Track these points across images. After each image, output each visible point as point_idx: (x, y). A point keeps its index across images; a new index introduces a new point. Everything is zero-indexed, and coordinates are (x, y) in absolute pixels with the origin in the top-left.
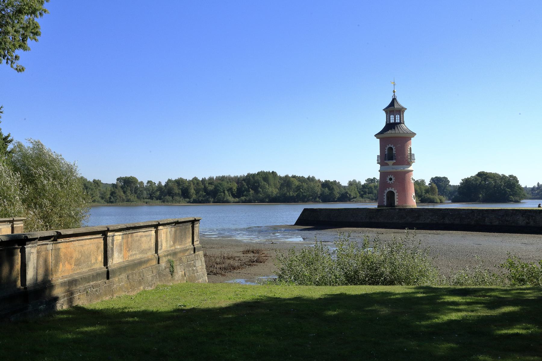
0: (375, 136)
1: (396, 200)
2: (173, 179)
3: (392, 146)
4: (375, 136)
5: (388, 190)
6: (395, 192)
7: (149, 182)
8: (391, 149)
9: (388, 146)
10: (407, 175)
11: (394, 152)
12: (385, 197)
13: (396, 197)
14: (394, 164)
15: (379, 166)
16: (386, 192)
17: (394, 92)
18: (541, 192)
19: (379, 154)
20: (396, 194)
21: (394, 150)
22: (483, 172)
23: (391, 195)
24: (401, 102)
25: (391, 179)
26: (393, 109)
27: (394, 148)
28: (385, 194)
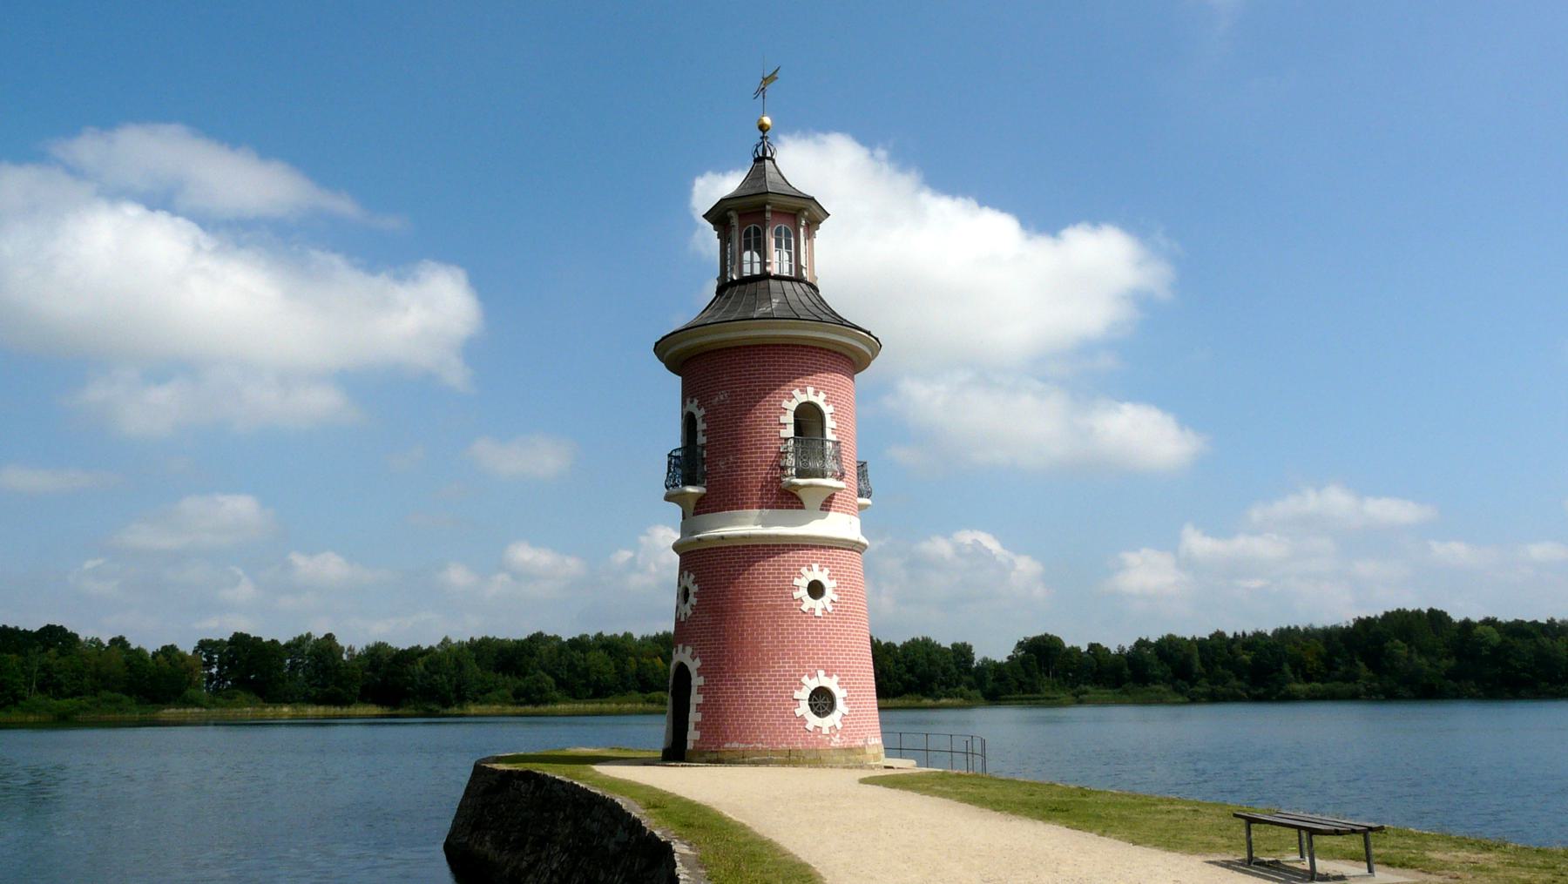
2: (1153, 640)
3: (693, 407)
6: (694, 666)
7: (1092, 646)
10: (766, 569)
11: (701, 440)
20: (697, 681)
21: (701, 426)
27: (699, 414)
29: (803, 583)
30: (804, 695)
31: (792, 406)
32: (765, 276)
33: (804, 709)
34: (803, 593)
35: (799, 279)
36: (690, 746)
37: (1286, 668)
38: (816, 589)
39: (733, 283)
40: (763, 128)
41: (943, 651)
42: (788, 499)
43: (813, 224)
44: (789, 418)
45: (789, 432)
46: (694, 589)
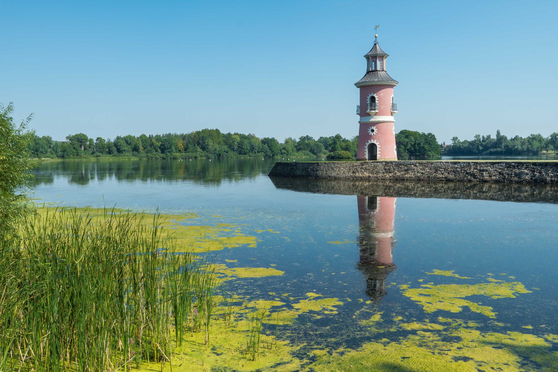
0: (355, 84)
1: (378, 152)
4: (355, 84)
6: (377, 144)
9: (370, 95)
11: (377, 102)
12: (367, 150)
13: (378, 149)
15: (359, 117)
16: (367, 144)
18: (557, 142)
19: (359, 104)
20: (378, 146)
21: (376, 99)
22: (406, 130)
25: (373, 131)
36: (378, 158)
37: (173, 148)
40: (376, 37)
41: (40, 139)
46: (375, 130)
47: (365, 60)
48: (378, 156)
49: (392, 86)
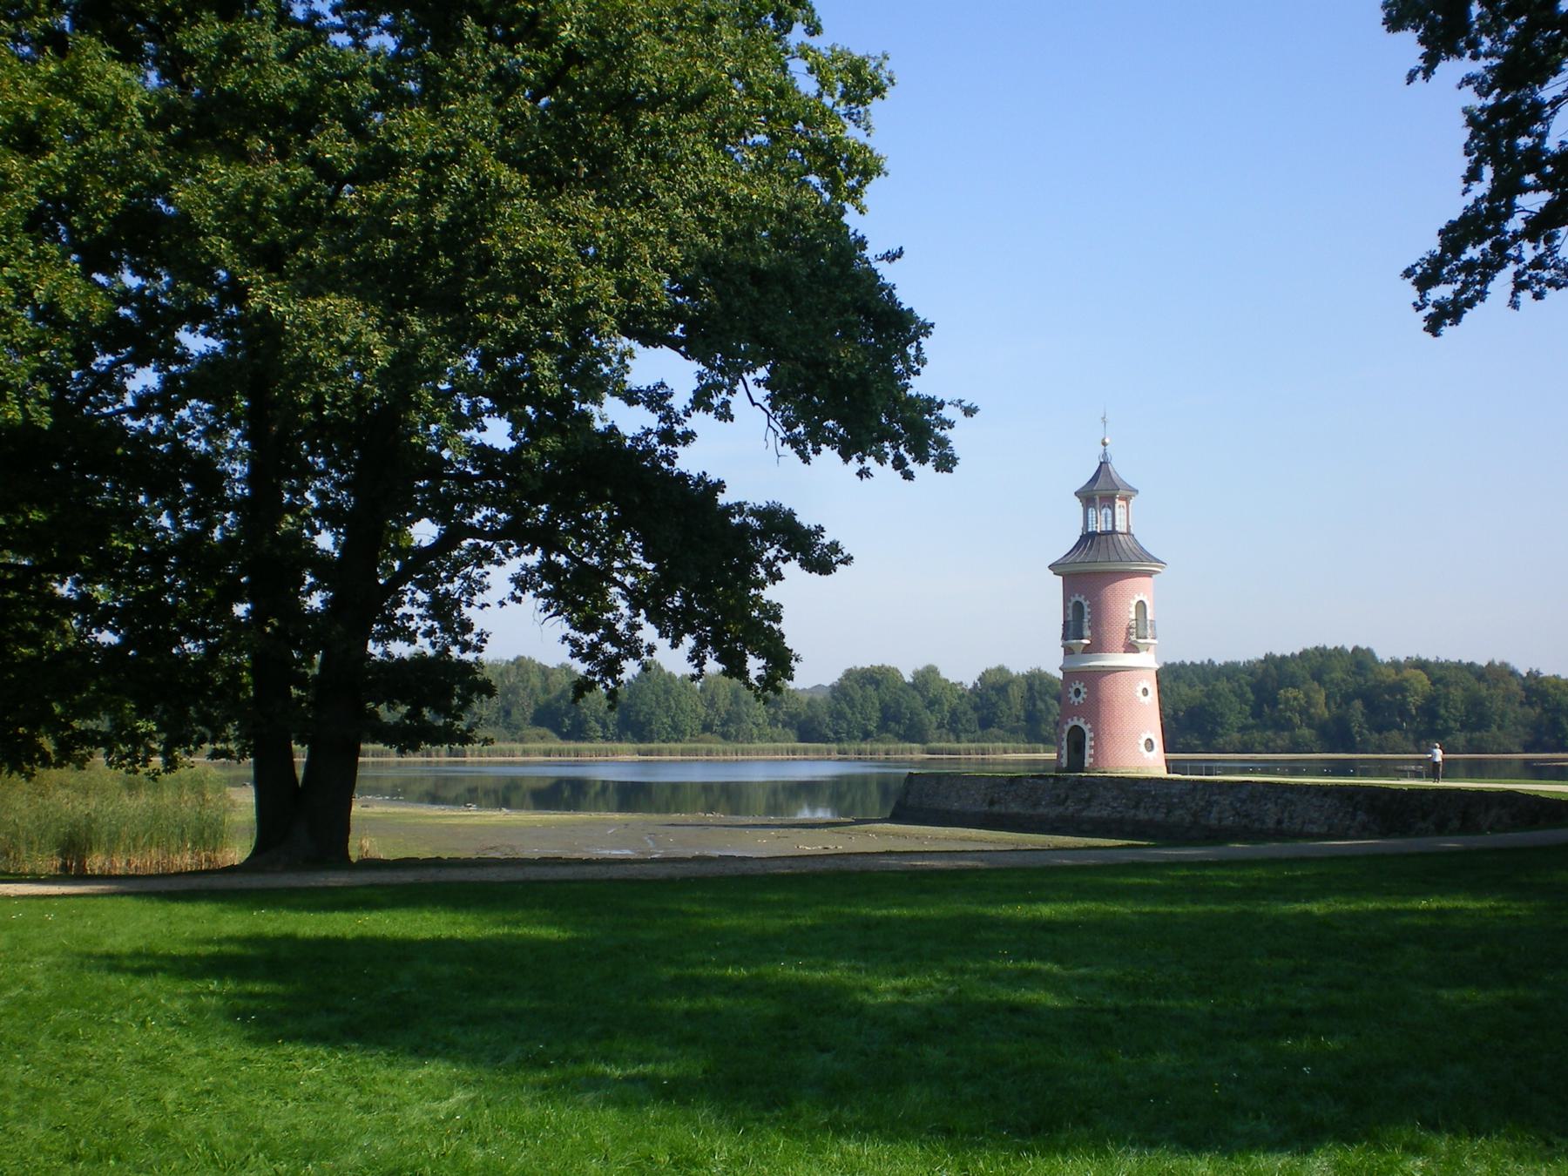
1: (1088, 752)
3: (1081, 599)
5: (1071, 723)
6: (1086, 728)
8: (1078, 606)
9: (1073, 600)
12: (1065, 744)
13: (1088, 743)
14: (1088, 650)
16: (1067, 728)
17: (1104, 444)
20: (1089, 735)
21: (1087, 610)
23: (1077, 741)
24: (1122, 470)
25: (1078, 692)
26: (1100, 491)
27: (1085, 604)
28: (1065, 736)
29: (1140, 689)
30: (1142, 742)
31: (1134, 603)
32: (1113, 532)
33: (1142, 748)
34: (1140, 694)
35: (1128, 533)
38: (1145, 692)
39: (1094, 534)
40: (1104, 444)
42: (1131, 648)
43: (1126, 499)
44: (1133, 609)
45: (1133, 616)
46: (1083, 690)
47: (1077, 505)
48: (1088, 761)
49: (1149, 574)
